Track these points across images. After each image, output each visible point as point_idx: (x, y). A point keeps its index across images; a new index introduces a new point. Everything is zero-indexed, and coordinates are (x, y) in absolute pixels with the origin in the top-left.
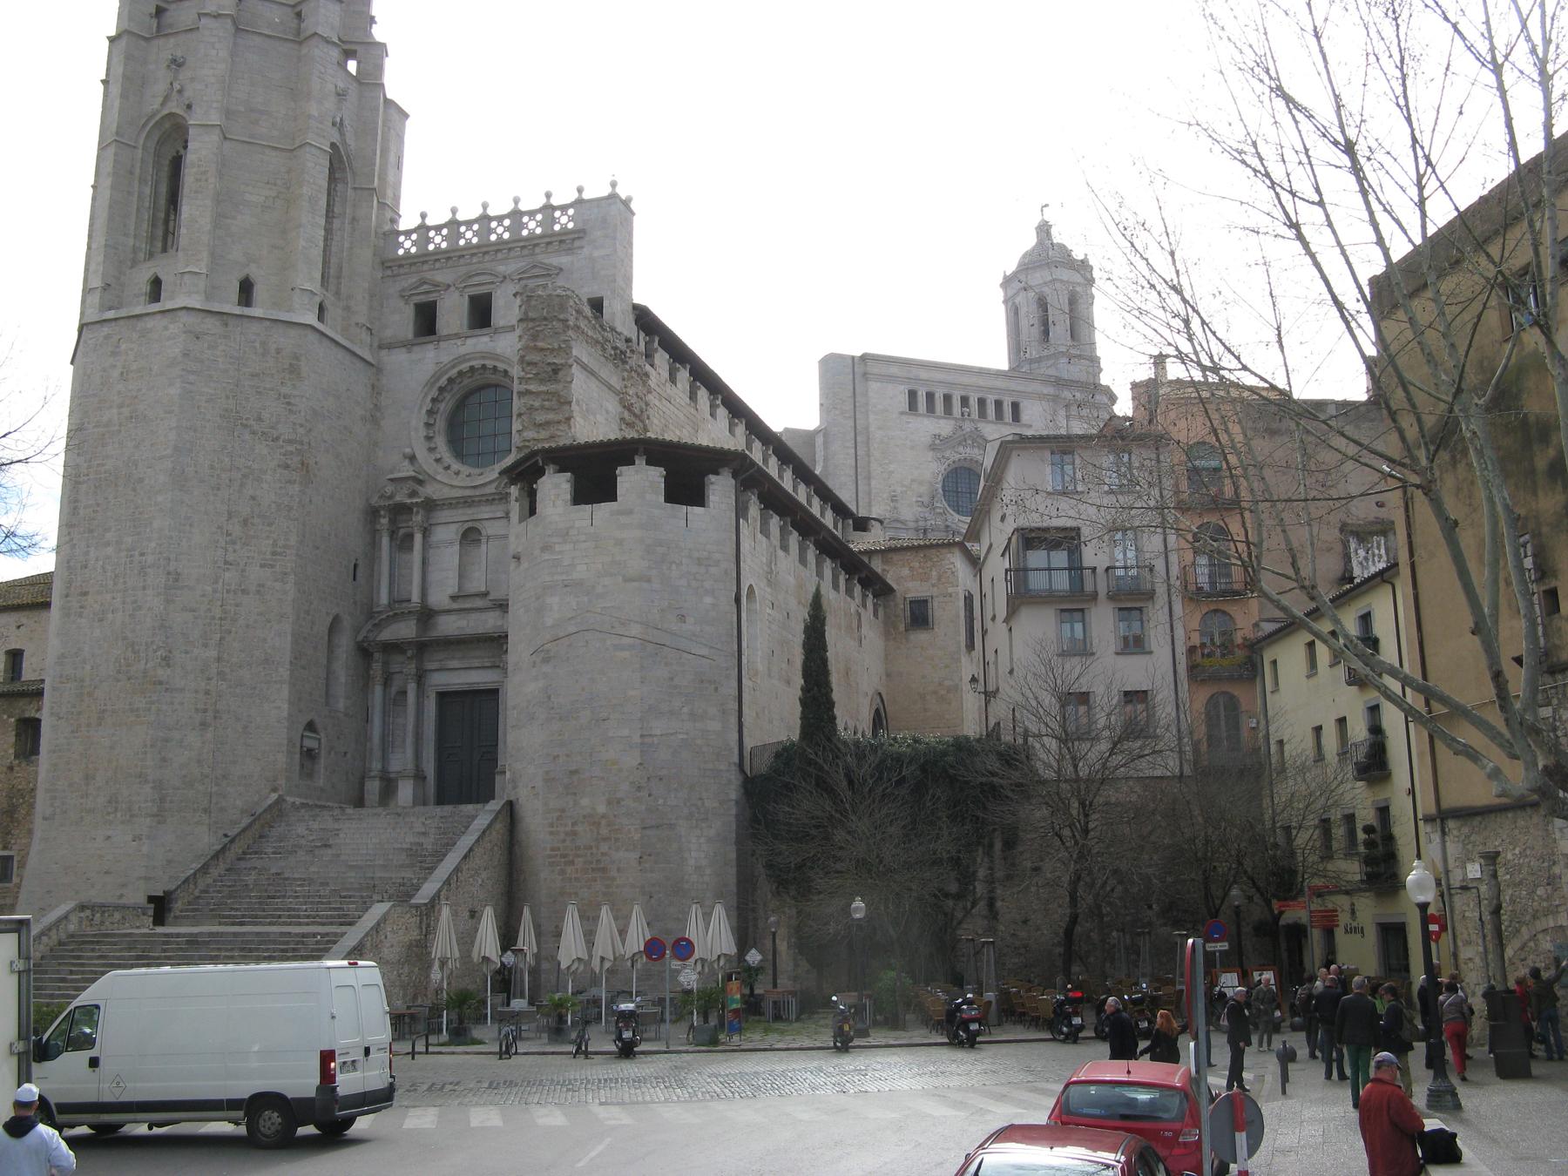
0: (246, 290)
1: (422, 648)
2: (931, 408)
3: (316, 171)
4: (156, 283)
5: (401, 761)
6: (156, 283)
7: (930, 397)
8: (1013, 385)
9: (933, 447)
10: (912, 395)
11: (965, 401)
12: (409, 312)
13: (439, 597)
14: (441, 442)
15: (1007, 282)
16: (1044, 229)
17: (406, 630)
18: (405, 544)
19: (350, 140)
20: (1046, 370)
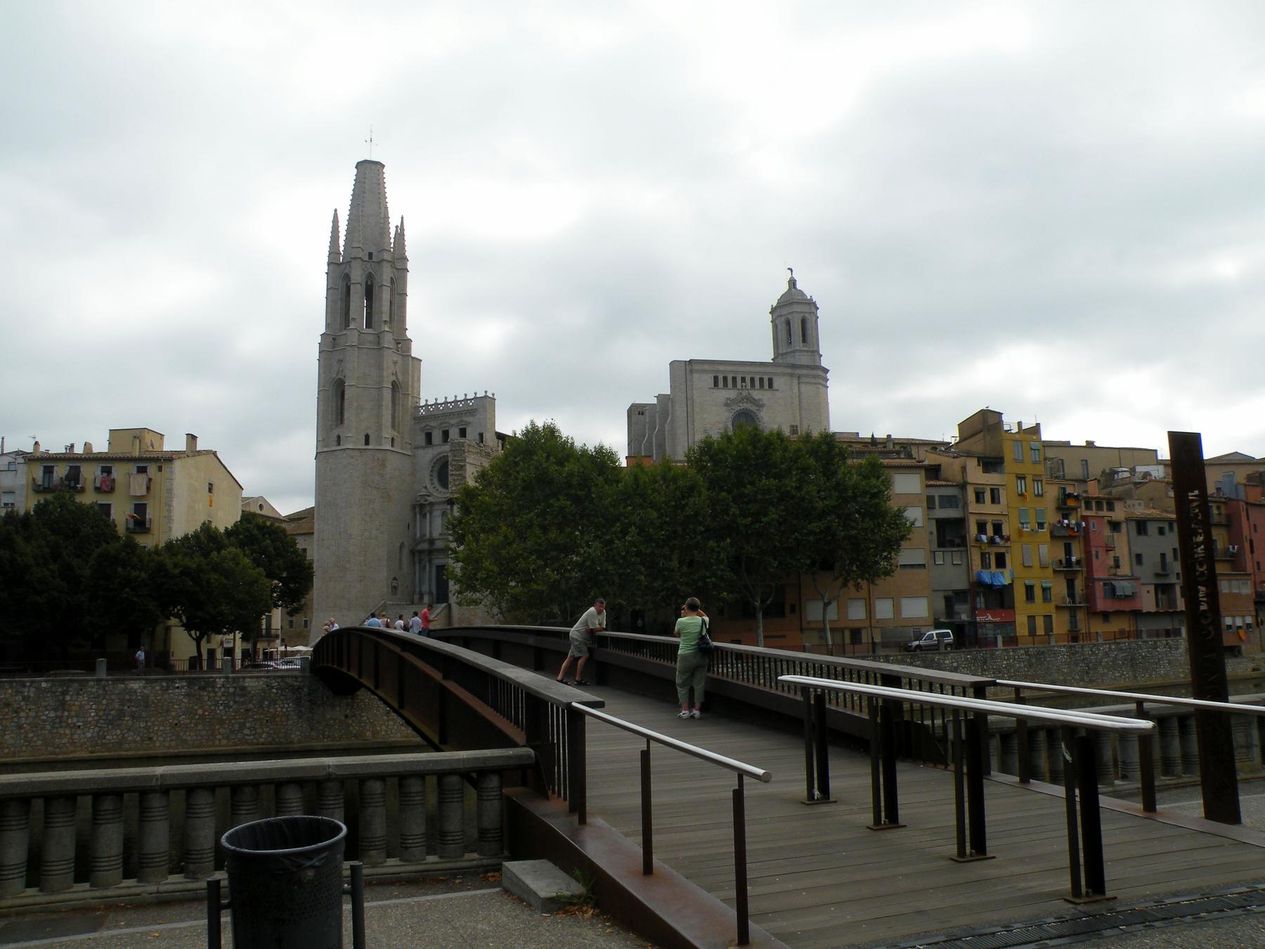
0: (367, 438)
1: (430, 552)
2: (725, 384)
3: (387, 395)
4: (339, 437)
5: (425, 588)
6: (339, 437)
7: (725, 379)
8: (769, 370)
9: (726, 405)
10: (716, 378)
11: (743, 379)
12: (423, 436)
13: (436, 535)
14: (435, 481)
15: (773, 311)
16: (792, 283)
17: (425, 546)
18: (424, 516)
19: (400, 378)
20: (790, 360)
